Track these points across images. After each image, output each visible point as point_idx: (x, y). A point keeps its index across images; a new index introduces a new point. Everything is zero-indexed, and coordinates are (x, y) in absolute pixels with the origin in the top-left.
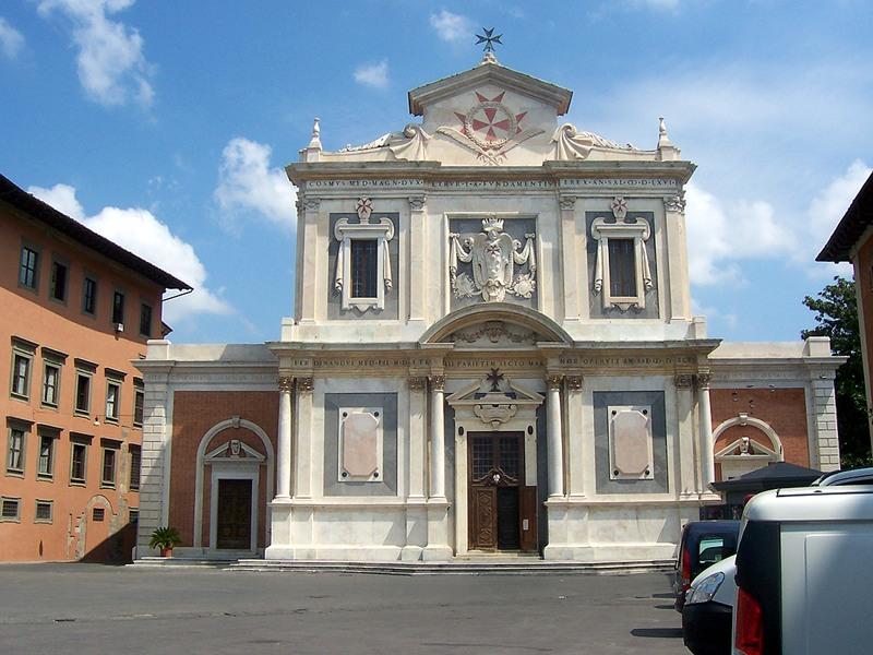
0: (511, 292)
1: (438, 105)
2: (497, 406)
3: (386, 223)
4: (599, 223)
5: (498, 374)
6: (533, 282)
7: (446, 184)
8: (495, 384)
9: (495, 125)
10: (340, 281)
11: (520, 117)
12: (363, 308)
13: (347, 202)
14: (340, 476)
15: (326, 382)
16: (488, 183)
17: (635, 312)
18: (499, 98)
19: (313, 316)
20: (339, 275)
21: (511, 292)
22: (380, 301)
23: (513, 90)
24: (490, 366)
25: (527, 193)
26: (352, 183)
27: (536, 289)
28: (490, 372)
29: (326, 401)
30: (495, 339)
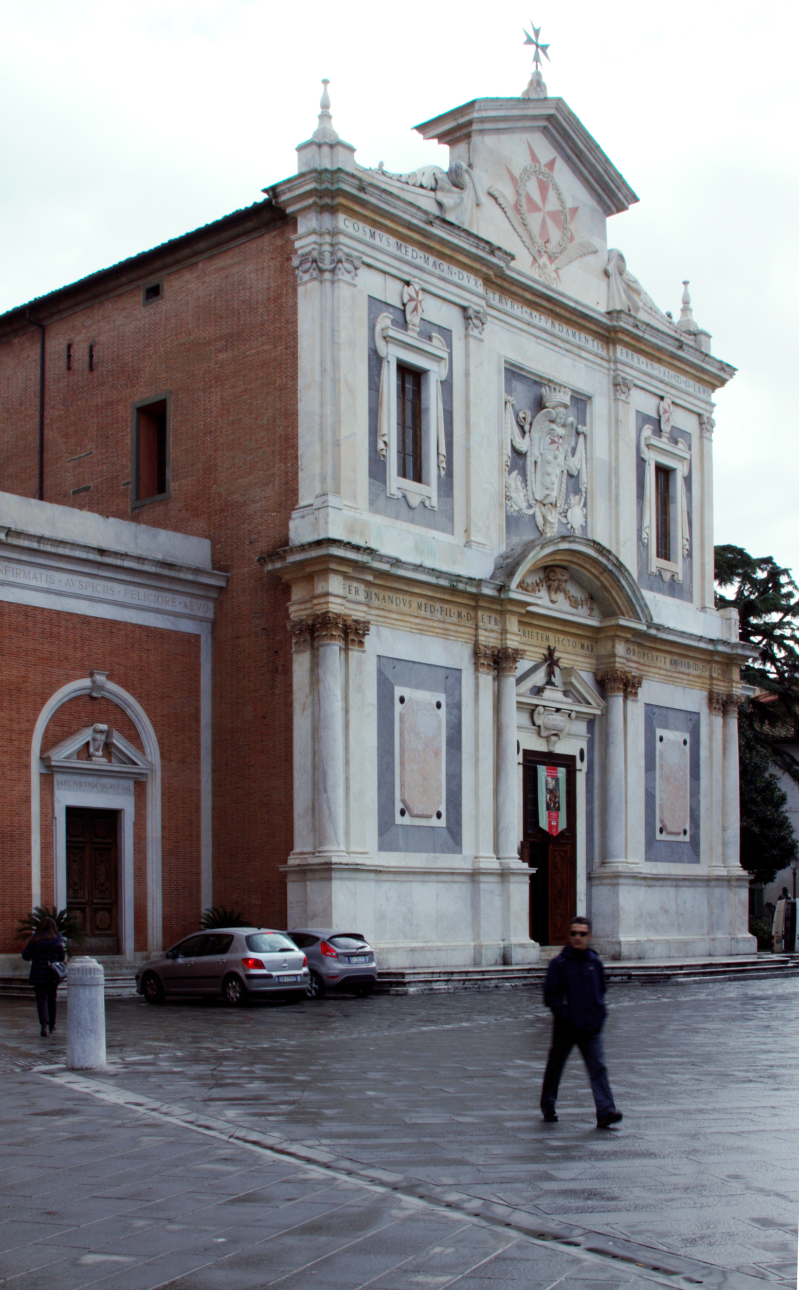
0: (564, 521)
1: (489, 140)
2: (558, 710)
3: (437, 346)
4: (647, 431)
5: (557, 655)
6: (584, 509)
7: (500, 300)
8: (550, 673)
9: (549, 213)
10: (386, 439)
11: (575, 210)
12: (415, 501)
13: (390, 281)
14: (397, 813)
15: (378, 634)
16: (543, 317)
17: (675, 589)
18: (551, 165)
19: (355, 497)
20: (384, 429)
21: (564, 521)
22: (430, 491)
23: (568, 159)
24: (546, 644)
25: (584, 354)
26: (399, 247)
27: (586, 522)
28: (546, 652)
29: (380, 672)
30: (554, 597)
